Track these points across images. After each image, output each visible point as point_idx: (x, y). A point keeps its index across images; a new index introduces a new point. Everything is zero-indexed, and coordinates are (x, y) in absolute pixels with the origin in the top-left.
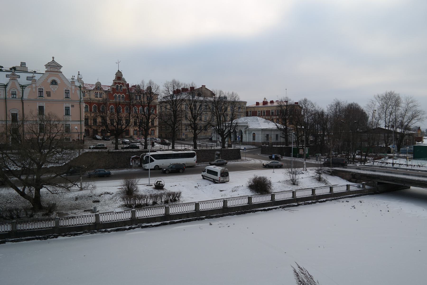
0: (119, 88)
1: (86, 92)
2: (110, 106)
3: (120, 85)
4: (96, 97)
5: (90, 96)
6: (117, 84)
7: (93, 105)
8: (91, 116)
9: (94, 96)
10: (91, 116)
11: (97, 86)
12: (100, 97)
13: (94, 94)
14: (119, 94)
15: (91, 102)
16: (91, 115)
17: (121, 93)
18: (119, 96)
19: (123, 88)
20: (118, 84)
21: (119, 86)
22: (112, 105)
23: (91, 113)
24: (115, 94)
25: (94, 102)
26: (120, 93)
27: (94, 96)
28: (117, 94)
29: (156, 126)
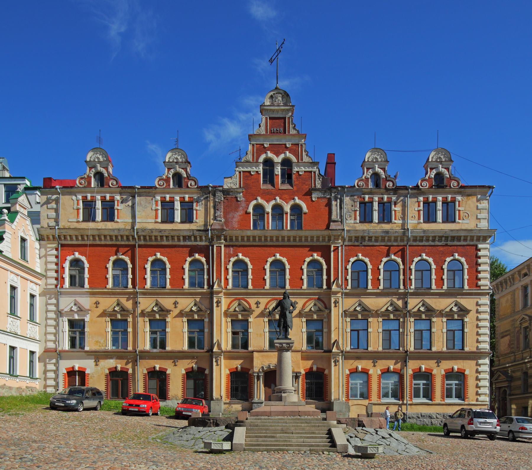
0: (278, 170)
3: (282, 156)
6: (270, 155)
9: (156, 217)
12: (182, 222)
13: (154, 207)
17: (287, 196)
18: (278, 209)
19: (298, 172)
20: (272, 152)
21: (278, 159)
22: (240, 255)
24: (254, 202)
26: (282, 194)
28: (268, 201)
29: (476, 356)
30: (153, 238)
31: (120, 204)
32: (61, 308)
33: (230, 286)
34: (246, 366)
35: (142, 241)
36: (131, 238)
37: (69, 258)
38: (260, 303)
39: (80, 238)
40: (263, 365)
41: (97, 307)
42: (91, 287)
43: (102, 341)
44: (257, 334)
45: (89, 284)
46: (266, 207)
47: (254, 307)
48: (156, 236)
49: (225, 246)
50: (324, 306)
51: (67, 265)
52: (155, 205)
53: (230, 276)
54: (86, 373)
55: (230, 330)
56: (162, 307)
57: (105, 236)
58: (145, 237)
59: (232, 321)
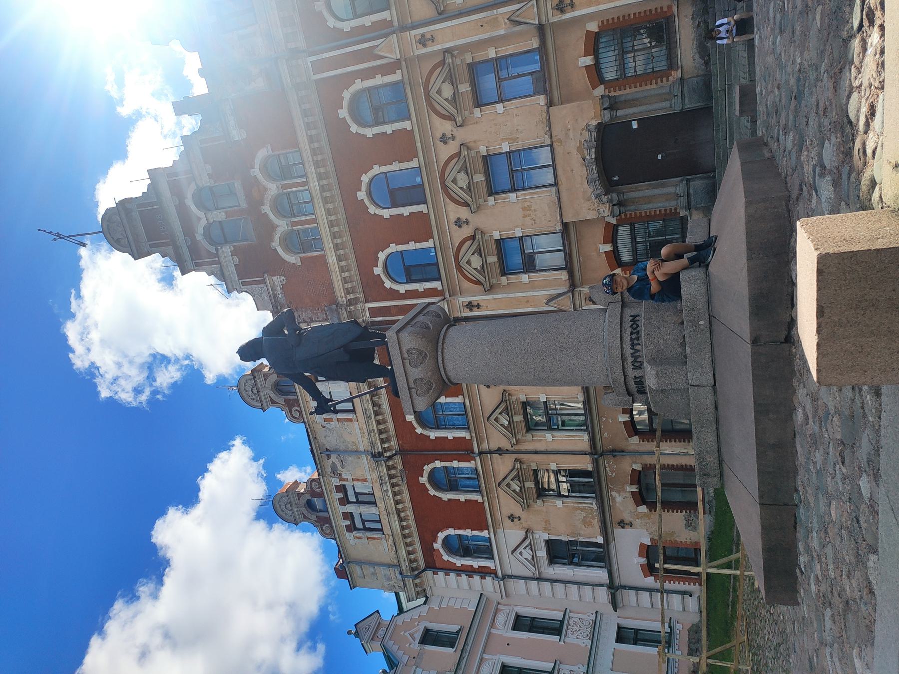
1: (341, 479)
2: (395, 295)
4: (353, 411)
5: (357, 452)
7: (419, 430)
8: (507, 452)
9: (350, 420)
10: (507, 452)
11: (273, 402)
13: (334, 424)
14: (266, 209)
15: (394, 443)
16: (500, 451)
19: (210, 177)
23: (480, 453)
24: (280, 250)
25: (391, 426)
27: (350, 420)
28: (273, 227)
30: (382, 427)
31: (344, 476)
32: (531, 575)
33: (436, 285)
34: (599, 232)
35: (392, 443)
36: (390, 463)
37: (446, 557)
38: (459, 219)
39: (409, 540)
40: (593, 197)
41: (519, 519)
42: (487, 528)
43: (584, 514)
44: (525, 216)
45: (481, 530)
46: (283, 229)
47: (467, 231)
48: (378, 423)
49: (367, 301)
50: (440, 69)
51: (459, 562)
52: (331, 423)
53: (420, 287)
54: (650, 544)
55: (525, 278)
56: (499, 411)
57: (397, 502)
58: (383, 441)
59: (504, 274)
